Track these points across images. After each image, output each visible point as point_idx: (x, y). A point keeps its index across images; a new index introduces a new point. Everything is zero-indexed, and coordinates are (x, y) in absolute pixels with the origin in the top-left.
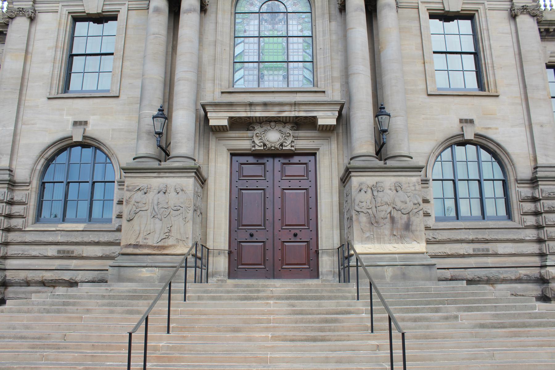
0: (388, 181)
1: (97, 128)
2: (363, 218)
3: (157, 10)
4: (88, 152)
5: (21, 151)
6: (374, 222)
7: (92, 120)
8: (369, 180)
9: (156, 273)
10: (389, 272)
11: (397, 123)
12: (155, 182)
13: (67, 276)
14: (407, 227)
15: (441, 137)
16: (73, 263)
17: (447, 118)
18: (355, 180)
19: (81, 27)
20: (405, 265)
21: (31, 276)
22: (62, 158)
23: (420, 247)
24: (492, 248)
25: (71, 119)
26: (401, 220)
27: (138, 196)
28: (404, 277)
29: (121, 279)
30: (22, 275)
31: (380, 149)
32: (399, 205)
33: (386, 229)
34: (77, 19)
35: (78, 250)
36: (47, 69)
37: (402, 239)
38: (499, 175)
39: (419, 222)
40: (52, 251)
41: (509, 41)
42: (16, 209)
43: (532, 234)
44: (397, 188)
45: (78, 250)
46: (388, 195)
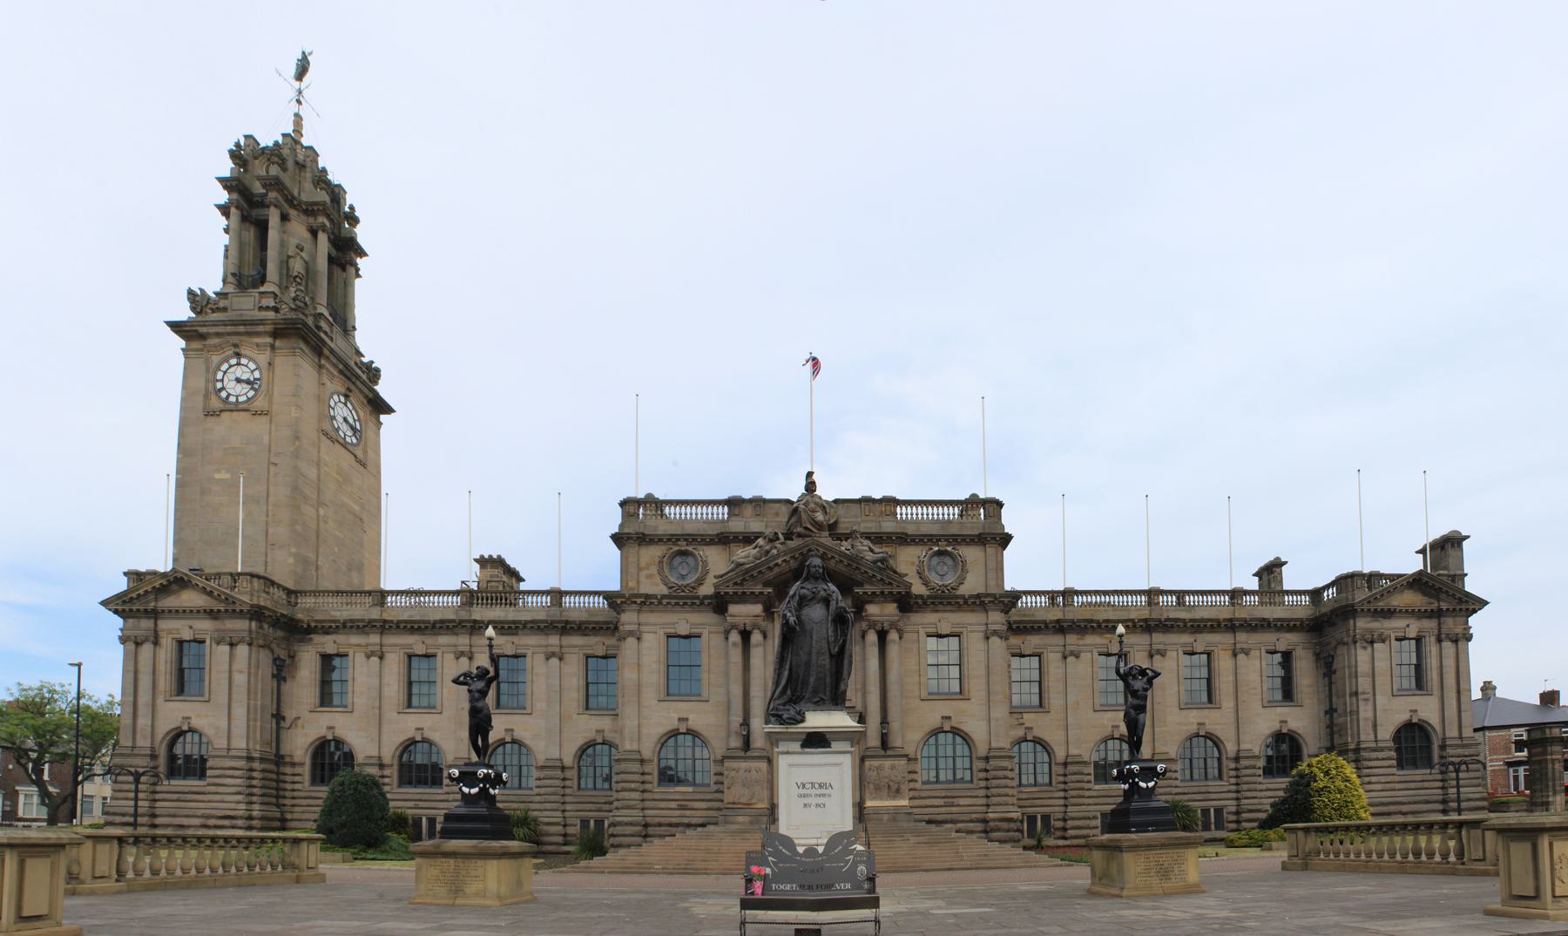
0: (887, 763)
1: (696, 722)
3: (735, 644)
4: (689, 737)
6: (878, 788)
7: (691, 717)
8: (876, 763)
9: (747, 819)
10: (886, 817)
11: (895, 725)
12: (743, 765)
13: (686, 821)
14: (898, 791)
15: (928, 729)
16: (688, 813)
17: (932, 715)
18: (867, 763)
20: (895, 813)
21: (662, 820)
22: (671, 742)
23: (905, 802)
24: (956, 801)
25: (676, 716)
26: (894, 787)
27: (733, 774)
28: (894, 820)
29: (726, 822)
31: (884, 742)
35: (691, 804)
36: (654, 678)
37: (894, 798)
38: (967, 753)
39: (905, 788)
40: (673, 805)
41: (982, 656)
42: (647, 778)
43: (982, 792)
44: (893, 767)
45: (691, 804)
46: (887, 772)
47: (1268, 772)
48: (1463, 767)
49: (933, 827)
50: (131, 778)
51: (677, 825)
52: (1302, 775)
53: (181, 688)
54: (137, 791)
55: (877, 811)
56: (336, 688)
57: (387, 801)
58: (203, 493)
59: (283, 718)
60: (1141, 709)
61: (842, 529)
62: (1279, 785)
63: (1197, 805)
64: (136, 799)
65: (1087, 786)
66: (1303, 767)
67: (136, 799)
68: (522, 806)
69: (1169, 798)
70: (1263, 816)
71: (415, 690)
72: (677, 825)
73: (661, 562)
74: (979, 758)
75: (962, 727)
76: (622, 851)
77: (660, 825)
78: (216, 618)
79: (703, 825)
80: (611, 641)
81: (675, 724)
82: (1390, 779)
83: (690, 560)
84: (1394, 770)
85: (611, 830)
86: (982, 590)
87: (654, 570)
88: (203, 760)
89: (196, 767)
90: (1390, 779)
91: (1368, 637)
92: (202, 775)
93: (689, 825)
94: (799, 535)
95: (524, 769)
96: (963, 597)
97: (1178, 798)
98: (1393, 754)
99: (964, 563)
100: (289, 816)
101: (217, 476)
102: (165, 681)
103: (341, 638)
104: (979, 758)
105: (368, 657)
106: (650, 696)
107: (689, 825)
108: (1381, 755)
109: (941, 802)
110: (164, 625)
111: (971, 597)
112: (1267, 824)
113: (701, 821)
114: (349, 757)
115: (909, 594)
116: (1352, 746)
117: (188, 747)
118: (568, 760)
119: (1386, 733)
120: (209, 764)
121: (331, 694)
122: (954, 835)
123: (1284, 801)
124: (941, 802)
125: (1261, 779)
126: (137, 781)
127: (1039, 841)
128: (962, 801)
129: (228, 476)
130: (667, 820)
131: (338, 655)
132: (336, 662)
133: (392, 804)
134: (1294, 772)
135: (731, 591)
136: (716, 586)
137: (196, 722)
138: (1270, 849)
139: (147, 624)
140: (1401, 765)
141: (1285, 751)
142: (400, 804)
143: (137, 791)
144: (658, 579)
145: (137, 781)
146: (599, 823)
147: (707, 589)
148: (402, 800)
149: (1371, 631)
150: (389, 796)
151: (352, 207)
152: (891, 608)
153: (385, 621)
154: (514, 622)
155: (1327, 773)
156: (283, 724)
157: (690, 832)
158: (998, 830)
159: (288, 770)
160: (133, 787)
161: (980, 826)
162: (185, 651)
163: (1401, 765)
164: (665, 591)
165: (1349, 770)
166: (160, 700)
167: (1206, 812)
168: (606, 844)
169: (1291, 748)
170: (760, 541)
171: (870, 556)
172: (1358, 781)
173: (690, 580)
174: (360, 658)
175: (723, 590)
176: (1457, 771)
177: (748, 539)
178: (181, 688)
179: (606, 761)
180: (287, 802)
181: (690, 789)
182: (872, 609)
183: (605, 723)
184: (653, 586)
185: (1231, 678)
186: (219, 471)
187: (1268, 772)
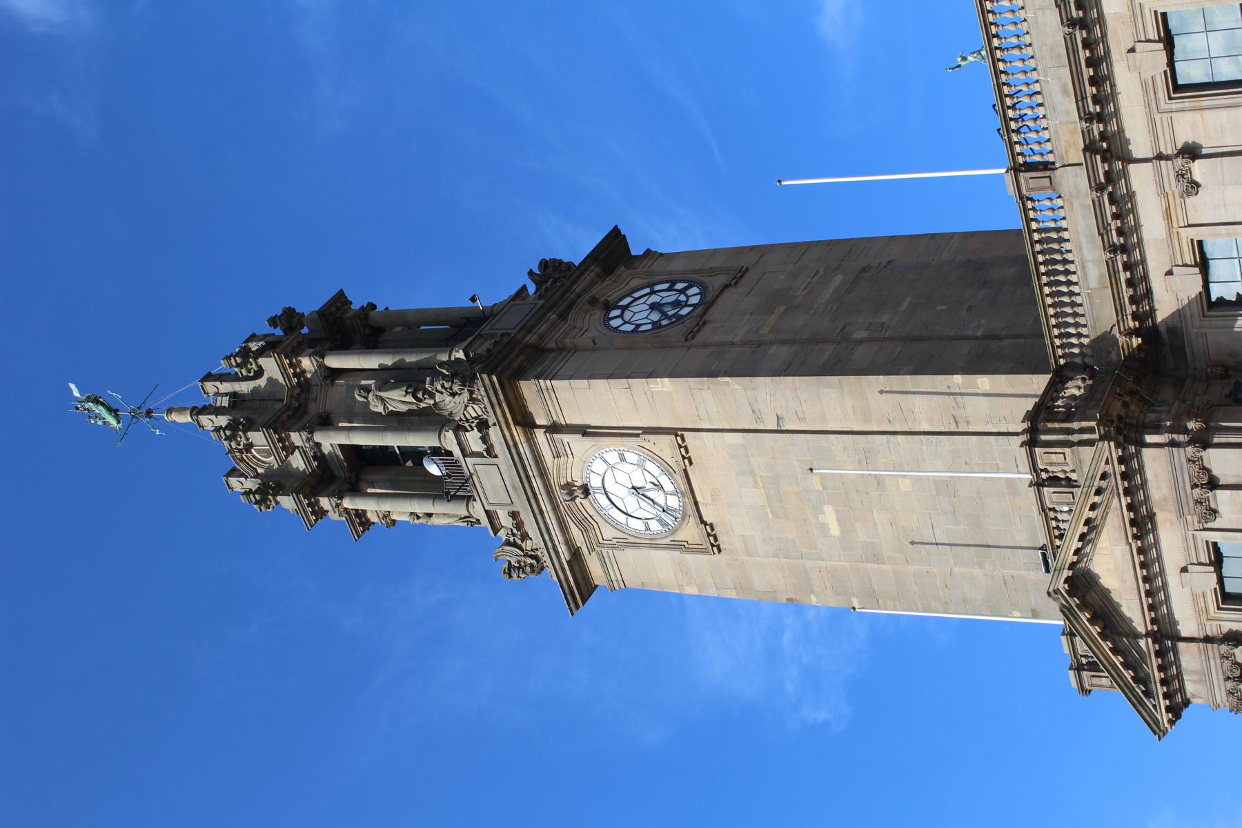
58: (876, 558)
78: (1151, 516)
103: (1156, 261)
105: (1194, 186)
129: (829, 510)
151: (273, 322)
153: (1090, 148)
174: (1201, 207)
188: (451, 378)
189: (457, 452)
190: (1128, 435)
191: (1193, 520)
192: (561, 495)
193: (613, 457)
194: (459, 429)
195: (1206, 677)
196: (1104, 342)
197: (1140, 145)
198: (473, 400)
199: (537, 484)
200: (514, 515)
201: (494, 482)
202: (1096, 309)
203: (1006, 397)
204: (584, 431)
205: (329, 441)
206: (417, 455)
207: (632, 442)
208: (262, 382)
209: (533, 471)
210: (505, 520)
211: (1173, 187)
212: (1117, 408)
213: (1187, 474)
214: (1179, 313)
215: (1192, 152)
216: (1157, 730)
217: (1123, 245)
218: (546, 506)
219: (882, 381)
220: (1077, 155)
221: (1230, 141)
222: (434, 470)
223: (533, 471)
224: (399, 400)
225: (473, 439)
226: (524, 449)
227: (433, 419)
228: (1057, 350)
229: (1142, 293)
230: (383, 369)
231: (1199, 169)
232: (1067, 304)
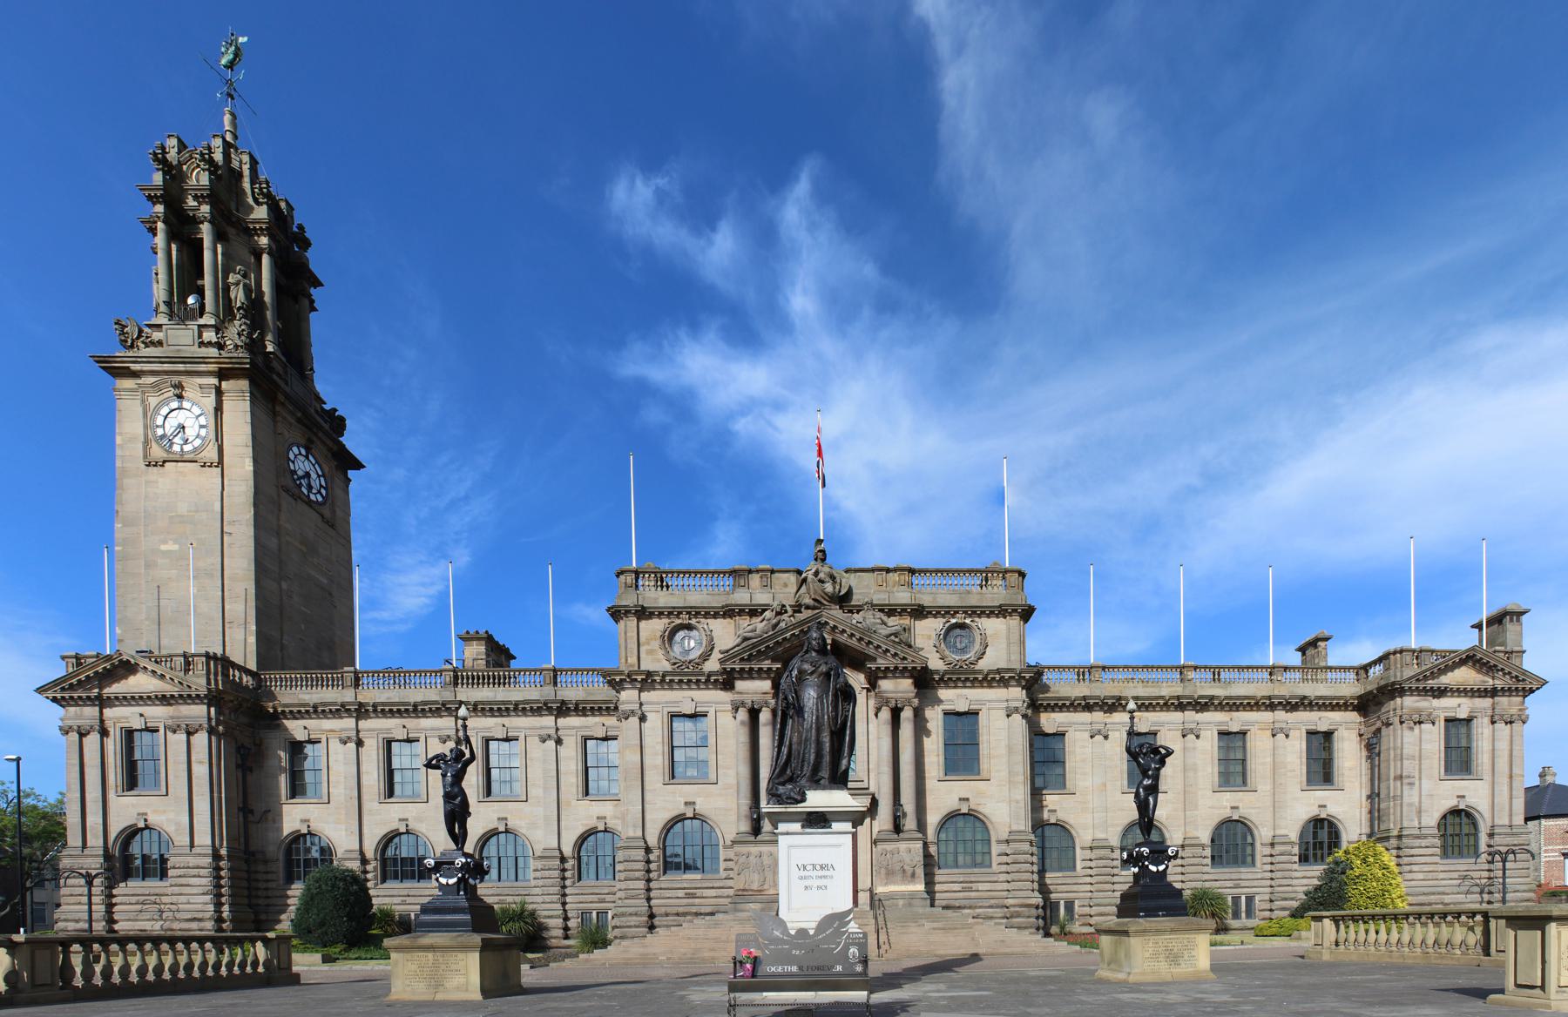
0: (903, 846)
1: (702, 806)
2: (883, 871)
5: (648, 825)
7: (699, 801)
8: (889, 847)
10: (901, 902)
12: (754, 849)
13: (694, 909)
14: (913, 875)
16: (697, 901)
19: (678, 725)
21: (669, 910)
25: (683, 800)
29: (736, 910)
30: (663, 910)
32: (907, 860)
33: (899, 877)
34: (673, 716)
40: (681, 893)
47: (1304, 859)
48: (1511, 857)
49: (949, 913)
50: (83, 881)
51: (685, 914)
52: (1337, 863)
53: (131, 781)
54: (90, 895)
55: (892, 896)
56: (309, 777)
57: (369, 898)
58: (148, 566)
59: (252, 812)
60: (1154, 790)
61: (856, 600)
62: (1312, 875)
63: (1229, 894)
64: (90, 904)
65: (1116, 871)
66: (1340, 854)
67: (90, 904)
68: (518, 899)
69: (1199, 885)
70: (1295, 904)
71: (397, 777)
72: (685, 914)
73: (662, 637)
74: (999, 842)
75: (980, 809)
76: (625, 943)
77: (667, 915)
79: (712, 914)
80: (611, 721)
81: (680, 809)
82: (1431, 868)
83: (694, 633)
84: (1437, 859)
85: (616, 922)
86: (1003, 665)
87: (656, 644)
88: (164, 860)
89: (157, 868)
90: (1431, 868)
91: (1416, 717)
92: (163, 874)
93: (697, 914)
94: (808, 607)
95: (521, 860)
96: (980, 672)
97: (1207, 885)
98: (1437, 842)
99: (984, 636)
100: (263, 917)
101: (163, 548)
102: (115, 776)
104: (999, 842)
106: (655, 777)
107: (697, 914)
108: (1424, 843)
109: (957, 887)
110: (108, 713)
111: (990, 672)
112: (1297, 914)
113: (708, 909)
114: (327, 852)
115: (925, 669)
116: (1395, 833)
117: (146, 846)
118: (568, 850)
119: (1431, 819)
120: (169, 864)
121: (303, 786)
122: (971, 920)
123: (1318, 888)
124: (957, 887)
125: (1296, 866)
126: (90, 884)
127: (1062, 928)
128: (981, 887)
129: (176, 547)
130: (675, 910)
131: (310, 742)
132: (309, 749)
133: (374, 901)
134: (1330, 859)
135: (737, 667)
136: (722, 661)
137: (153, 819)
138: (1299, 938)
139: (91, 712)
140: (1445, 854)
141: (1320, 837)
142: (387, 900)
143: (90, 895)
144: (660, 653)
145: (90, 884)
146: (602, 914)
147: (713, 665)
148: (388, 896)
149: (1419, 711)
150: (371, 892)
152: (906, 685)
154: (503, 703)
155: (1364, 861)
156: (251, 818)
157: (698, 921)
158: (1018, 915)
159: (261, 868)
160: (86, 890)
161: (999, 912)
162: (137, 742)
163: (1445, 854)
164: (668, 667)
165: (1388, 858)
166: (111, 795)
167: (1236, 899)
168: (610, 936)
169: (1330, 833)
170: (768, 614)
171: (884, 631)
172: (1396, 870)
173: (694, 655)
175: (729, 666)
176: (1504, 861)
177: (754, 612)
178: (131, 781)
179: (609, 851)
180: (261, 901)
181: (699, 876)
182: (885, 685)
183: (607, 809)
184: (656, 662)
185: (1269, 760)
186: (165, 542)
187: (1304, 859)
188: (250, 336)
189: (202, 321)
190: (212, 699)
191: (170, 722)
192: (176, 379)
193: (202, 421)
194: (217, 329)
195: (78, 717)
196: (272, 697)
197: (363, 724)
198: (236, 346)
199: (181, 367)
200: (160, 343)
201: (181, 338)
202: (289, 694)
203: (243, 648)
204: (219, 409)
205: (206, 232)
206: (200, 292)
207: (212, 436)
208: (250, 200)
209: (189, 367)
210: (157, 336)
211: (344, 735)
212: (227, 697)
213: (195, 723)
214: (286, 729)
215: (360, 743)
216: (41, 690)
217: (316, 711)
218: (166, 367)
219: (252, 591)
220: (361, 699)
221: (363, 758)
222: (191, 300)
223: (189, 367)
224: (238, 295)
225: (209, 336)
226: (202, 368)
227: (227, 312)
228: (269, 676)
229: (296, 716)
230: (260, 293)
231: (352, 746)
232: (292, 684)
